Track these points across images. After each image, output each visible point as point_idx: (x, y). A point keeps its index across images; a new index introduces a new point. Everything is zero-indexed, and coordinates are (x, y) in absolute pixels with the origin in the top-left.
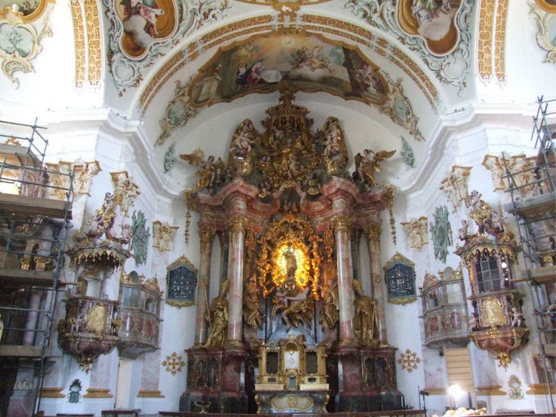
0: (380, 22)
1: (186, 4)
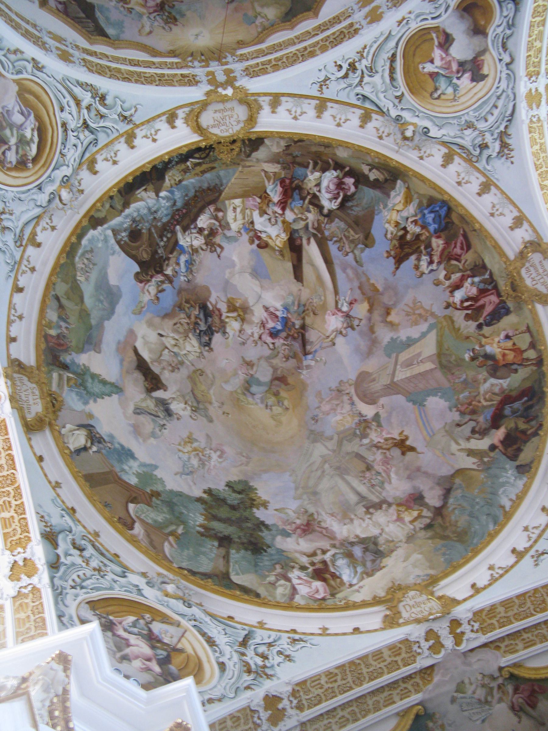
0: (78, 91)
1: (384, 82)
